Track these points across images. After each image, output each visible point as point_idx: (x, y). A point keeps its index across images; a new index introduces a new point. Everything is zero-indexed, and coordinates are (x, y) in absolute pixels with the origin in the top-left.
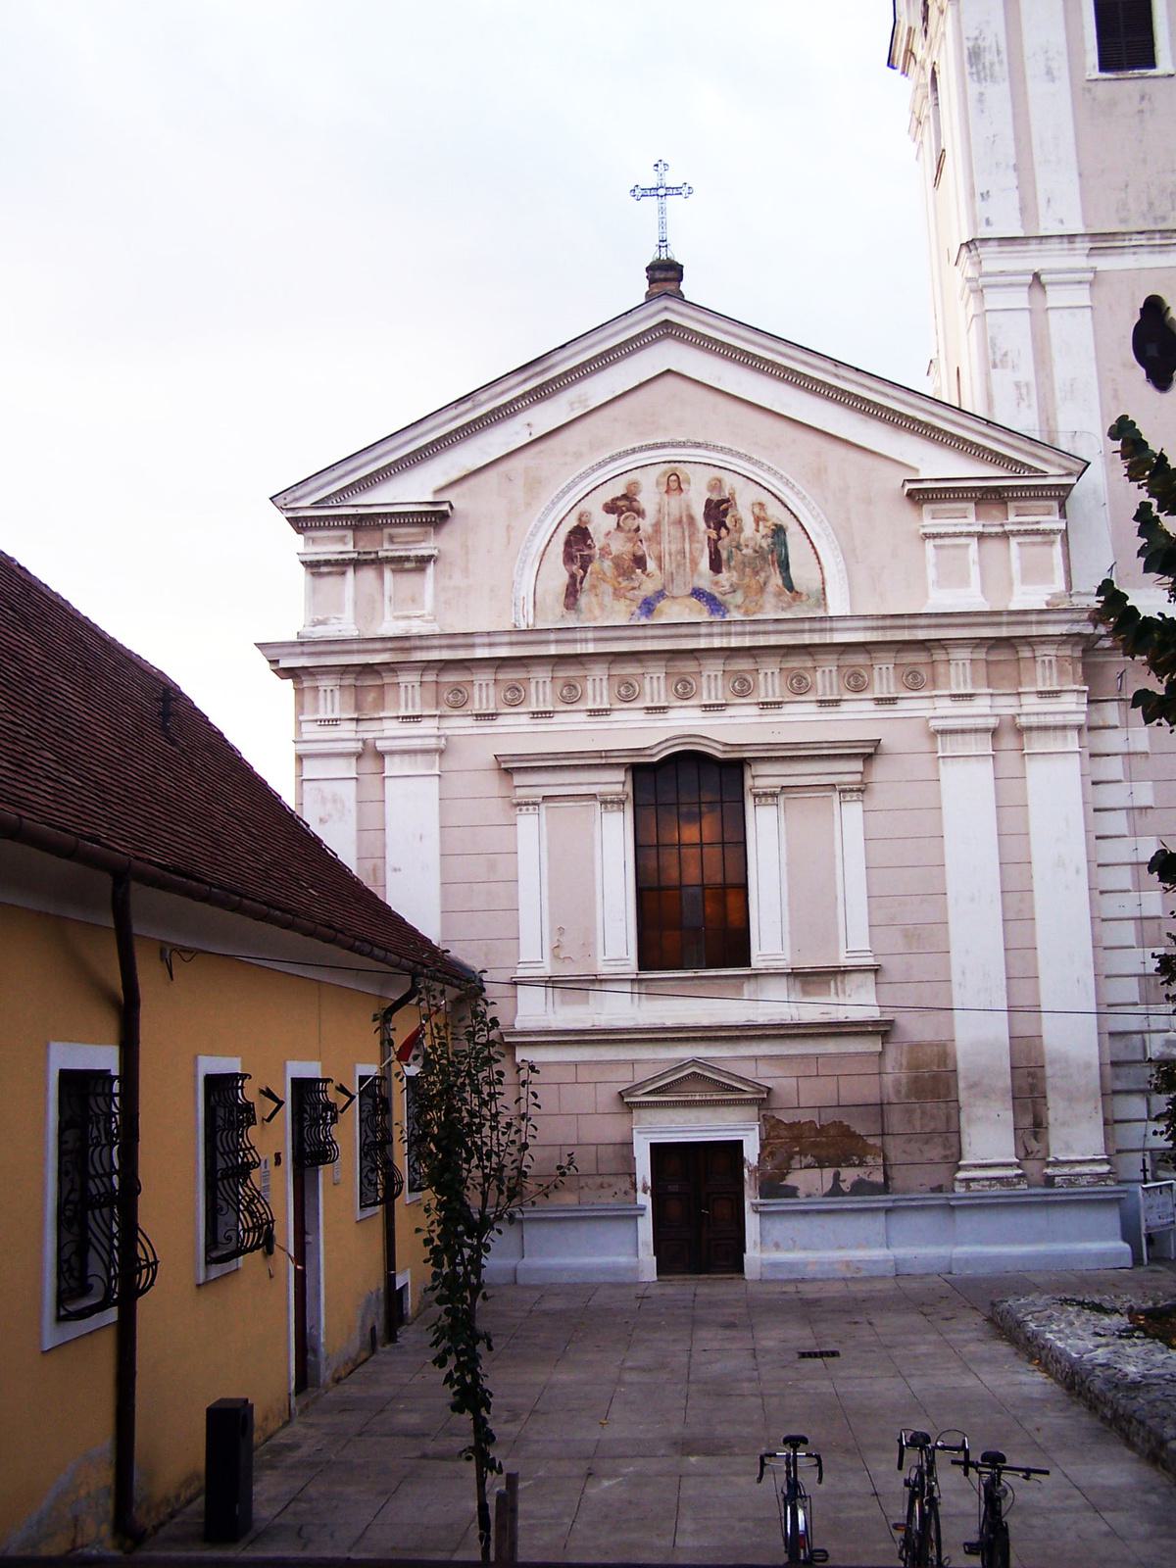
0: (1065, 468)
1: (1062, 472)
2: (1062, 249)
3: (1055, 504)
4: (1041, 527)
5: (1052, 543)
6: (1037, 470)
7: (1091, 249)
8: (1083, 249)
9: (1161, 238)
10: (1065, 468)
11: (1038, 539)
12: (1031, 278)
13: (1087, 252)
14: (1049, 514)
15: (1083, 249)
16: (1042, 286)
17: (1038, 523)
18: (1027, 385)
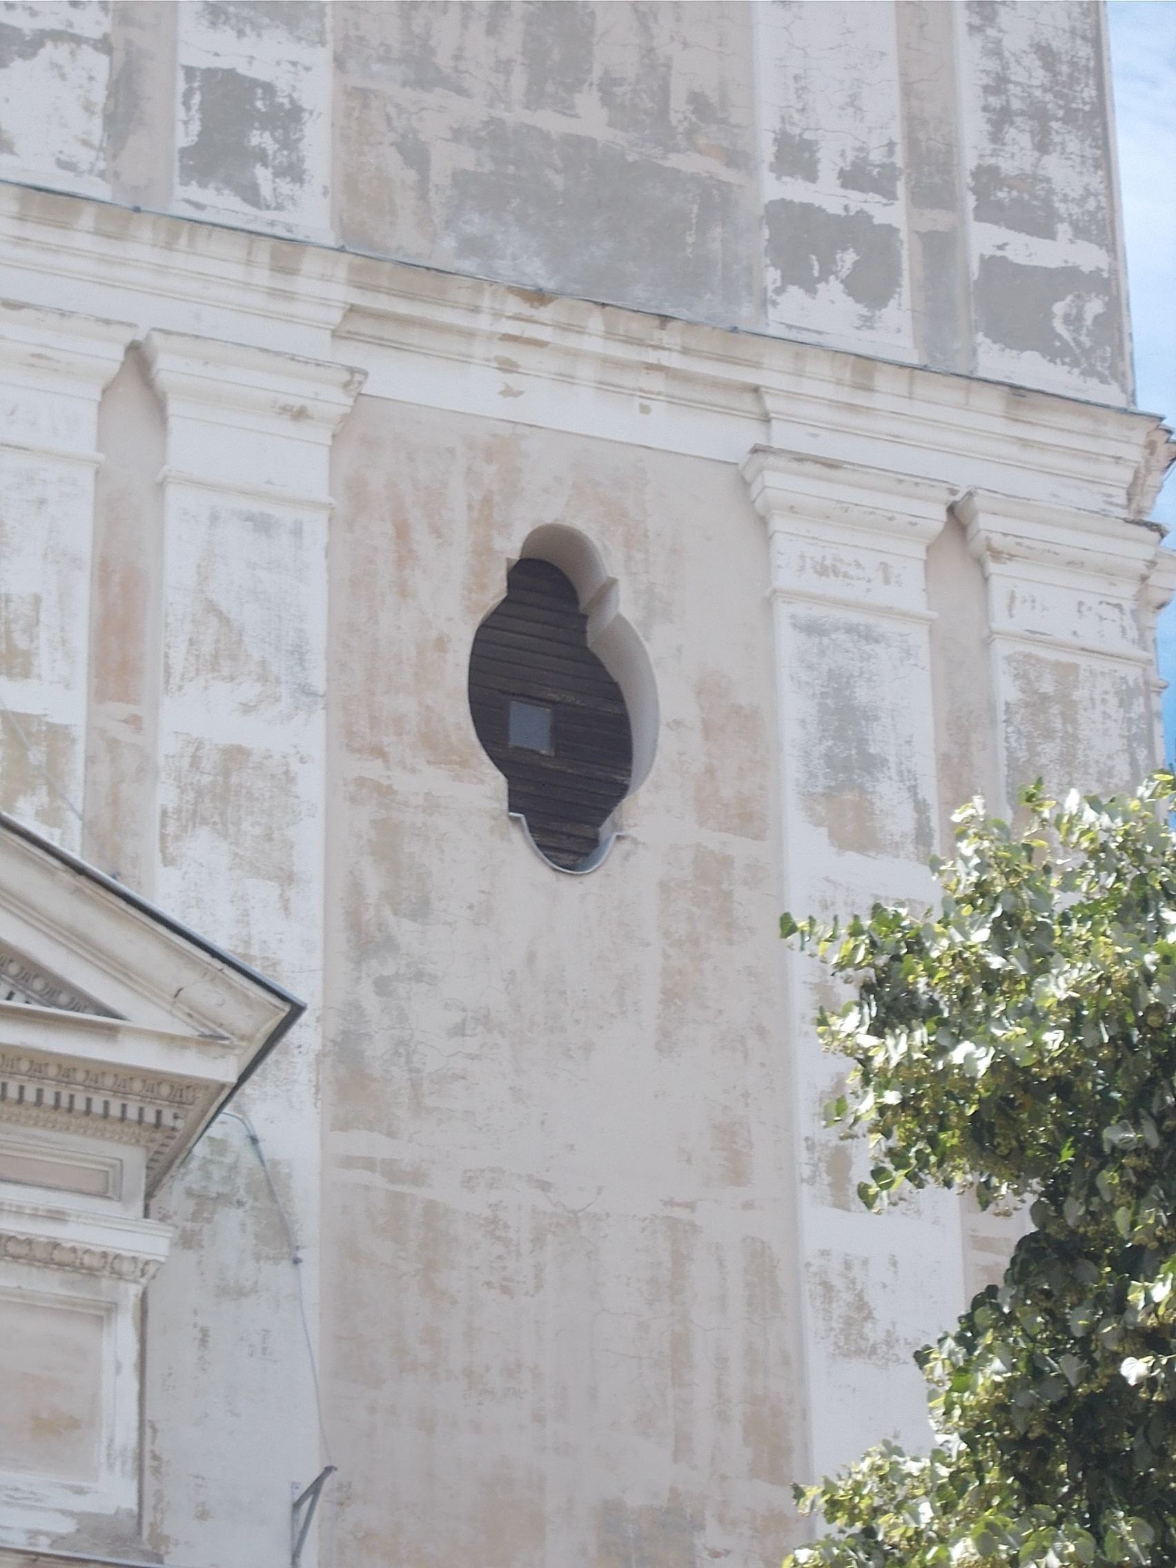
0: (194, 1014)
1: (179, 1028)
2: (247, 286)
3: (133, 1159)
4: (68, 1234)
5: (104, 1314)
6: (81, 1001)
7: (353, 310)
8: (325, 302)
9: (609, 335)
10: (194, 1014)
11: (49, 1284)
12: (118, 354)
13: (336, 316)
14: (103, 1195)
15: (325, 302)
16: (157, 405)
17: (57, 1216)
18: (57, 735)
